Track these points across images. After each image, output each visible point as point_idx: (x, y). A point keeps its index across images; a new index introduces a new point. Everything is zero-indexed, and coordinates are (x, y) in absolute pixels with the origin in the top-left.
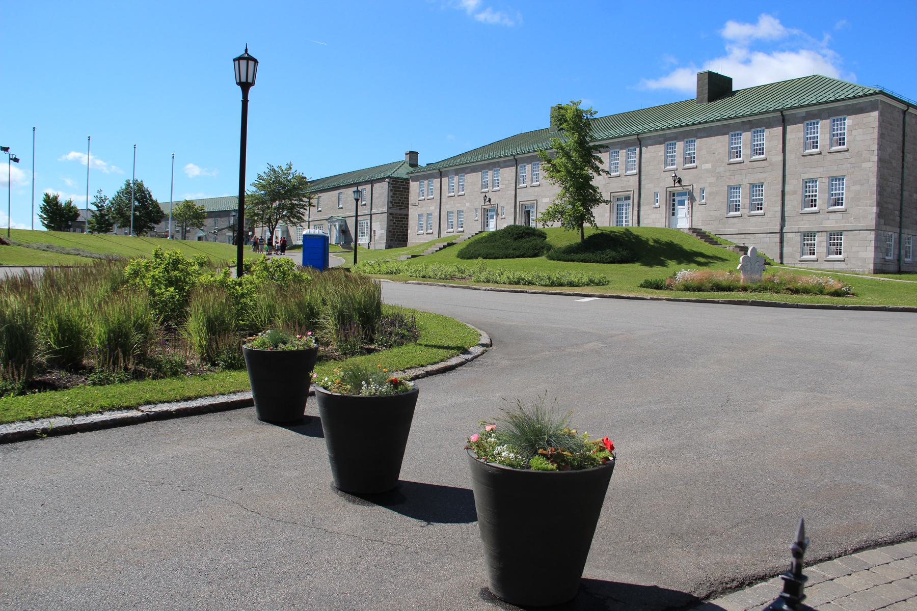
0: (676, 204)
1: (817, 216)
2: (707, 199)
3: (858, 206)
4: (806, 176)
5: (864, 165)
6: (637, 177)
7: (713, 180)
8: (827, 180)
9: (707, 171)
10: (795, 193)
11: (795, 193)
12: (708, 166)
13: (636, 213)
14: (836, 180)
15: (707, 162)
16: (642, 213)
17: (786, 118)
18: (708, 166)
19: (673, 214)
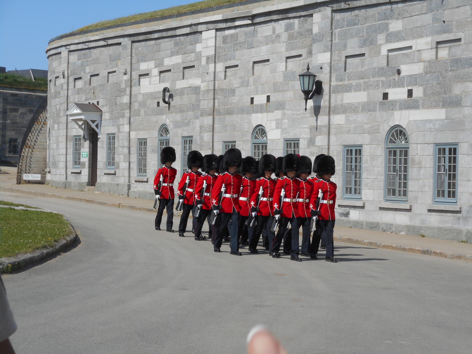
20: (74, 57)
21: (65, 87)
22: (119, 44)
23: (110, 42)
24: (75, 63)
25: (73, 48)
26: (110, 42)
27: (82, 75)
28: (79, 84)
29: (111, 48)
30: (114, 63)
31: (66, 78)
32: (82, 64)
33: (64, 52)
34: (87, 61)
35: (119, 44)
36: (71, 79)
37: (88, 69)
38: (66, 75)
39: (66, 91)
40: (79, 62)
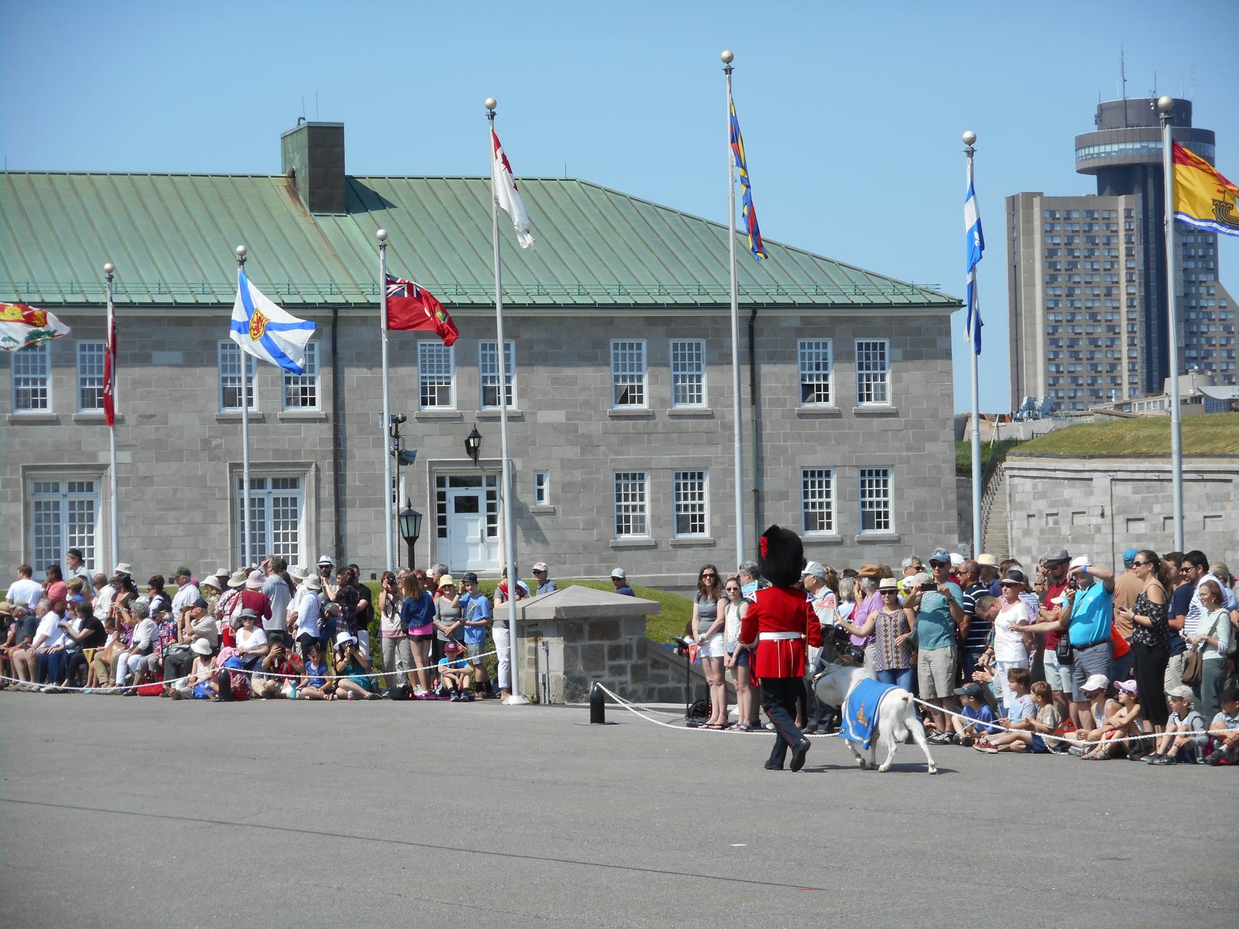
0: (451, 506)
1: (835, 551)
2: (553, 498)
3: (922, 530)
4: (815, 460)
5: (930, 447)
6: (327, 430)
7: (573, 452)
8: (857, 473)
9: (555, 428)
10: (783, 496)
11: (783, 496)
12: (558, 416)
13: (328, 529)
14: (873, 476)
15: (553, 405)
16: (351, 528)
17: (758, 325)
18: (558, 416)
19: (443, 533)
20: (1120, 489)
21: (1106, 530)
22: (1230, 481)
23: (1206, 476)
24: (1127, 498)
25: (1120, 475)
26: (1206, 476)
27: (1144, 514)
28: (1139, 528)
29: (1209, 484)
30: (1219, 504)
31: (1108, 520)
32: (1144, 500)
33: (1101, 481)
34: (1157, 497)
35: (1230, 481)
36: (1119, 520)
37: (1157, 508)
38: (1108, 512)
39: (1110, 537)
40: (1138, 497)
